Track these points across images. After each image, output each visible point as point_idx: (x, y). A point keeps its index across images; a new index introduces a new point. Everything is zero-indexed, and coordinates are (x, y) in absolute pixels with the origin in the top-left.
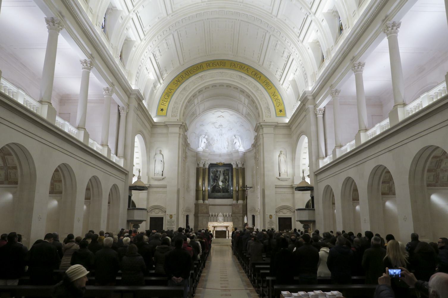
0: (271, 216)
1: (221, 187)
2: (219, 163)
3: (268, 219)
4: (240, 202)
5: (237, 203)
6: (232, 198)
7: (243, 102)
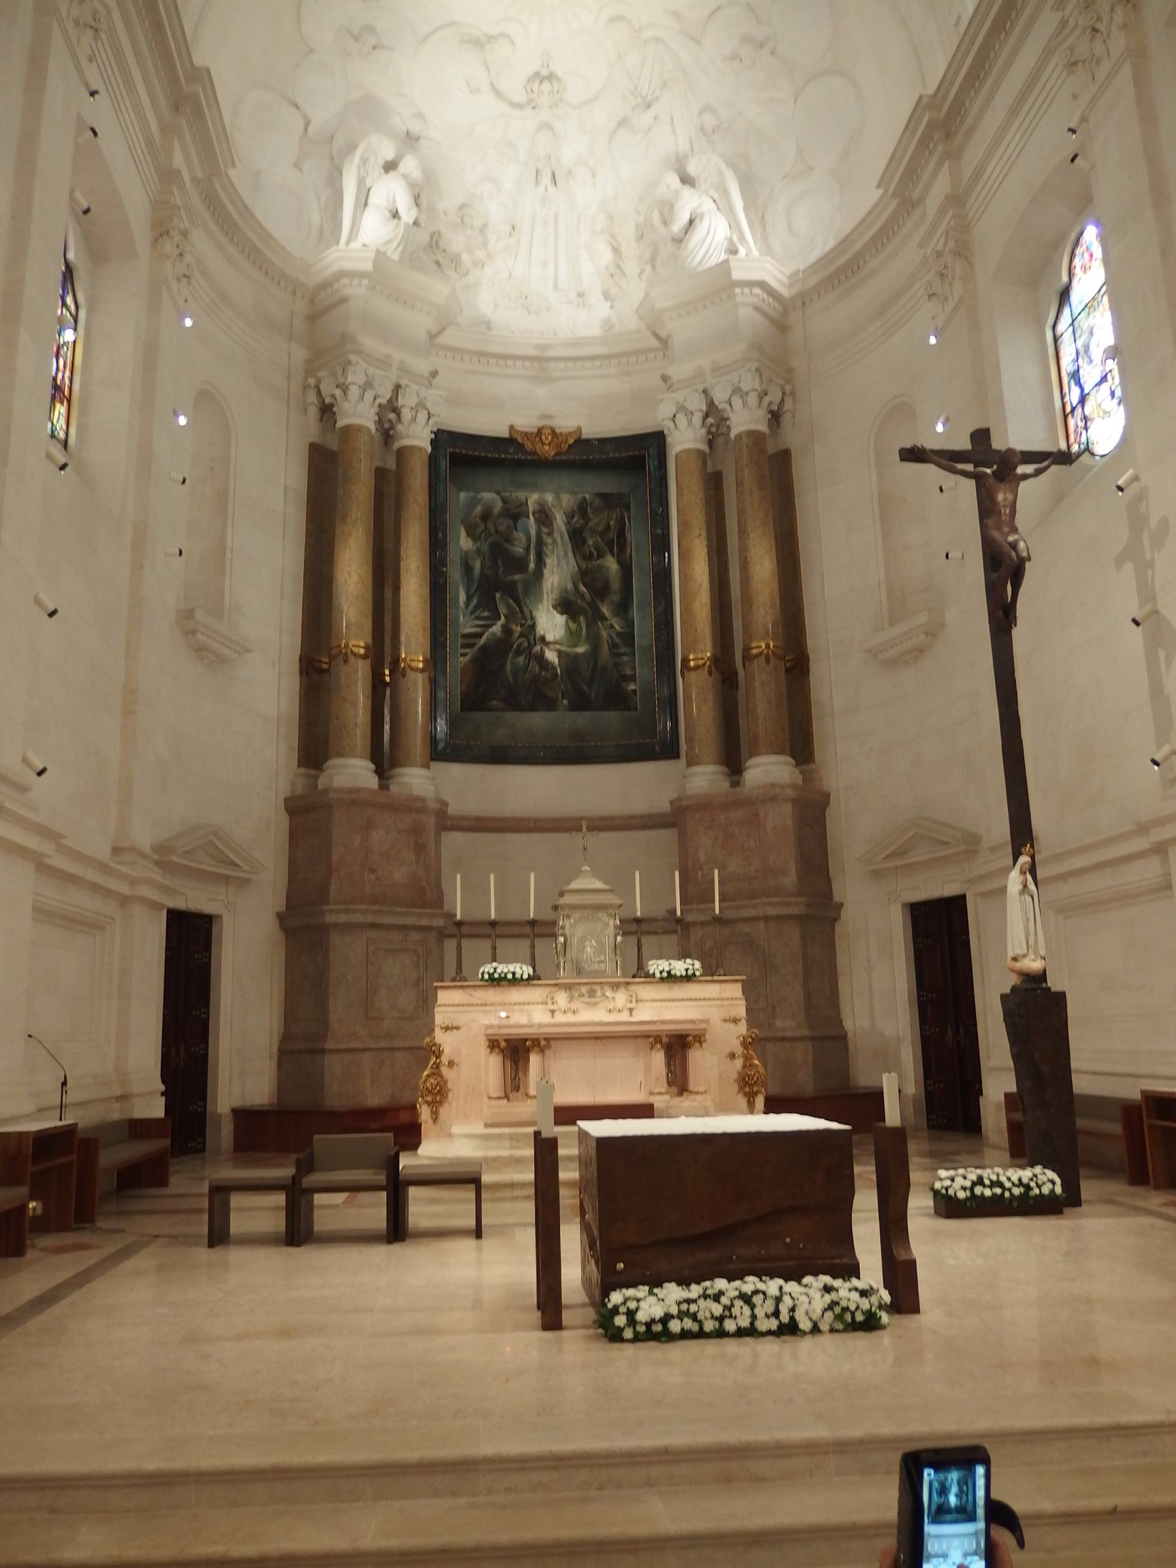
1: (551, 656)
5: (735, 784)
6: (669, 750)
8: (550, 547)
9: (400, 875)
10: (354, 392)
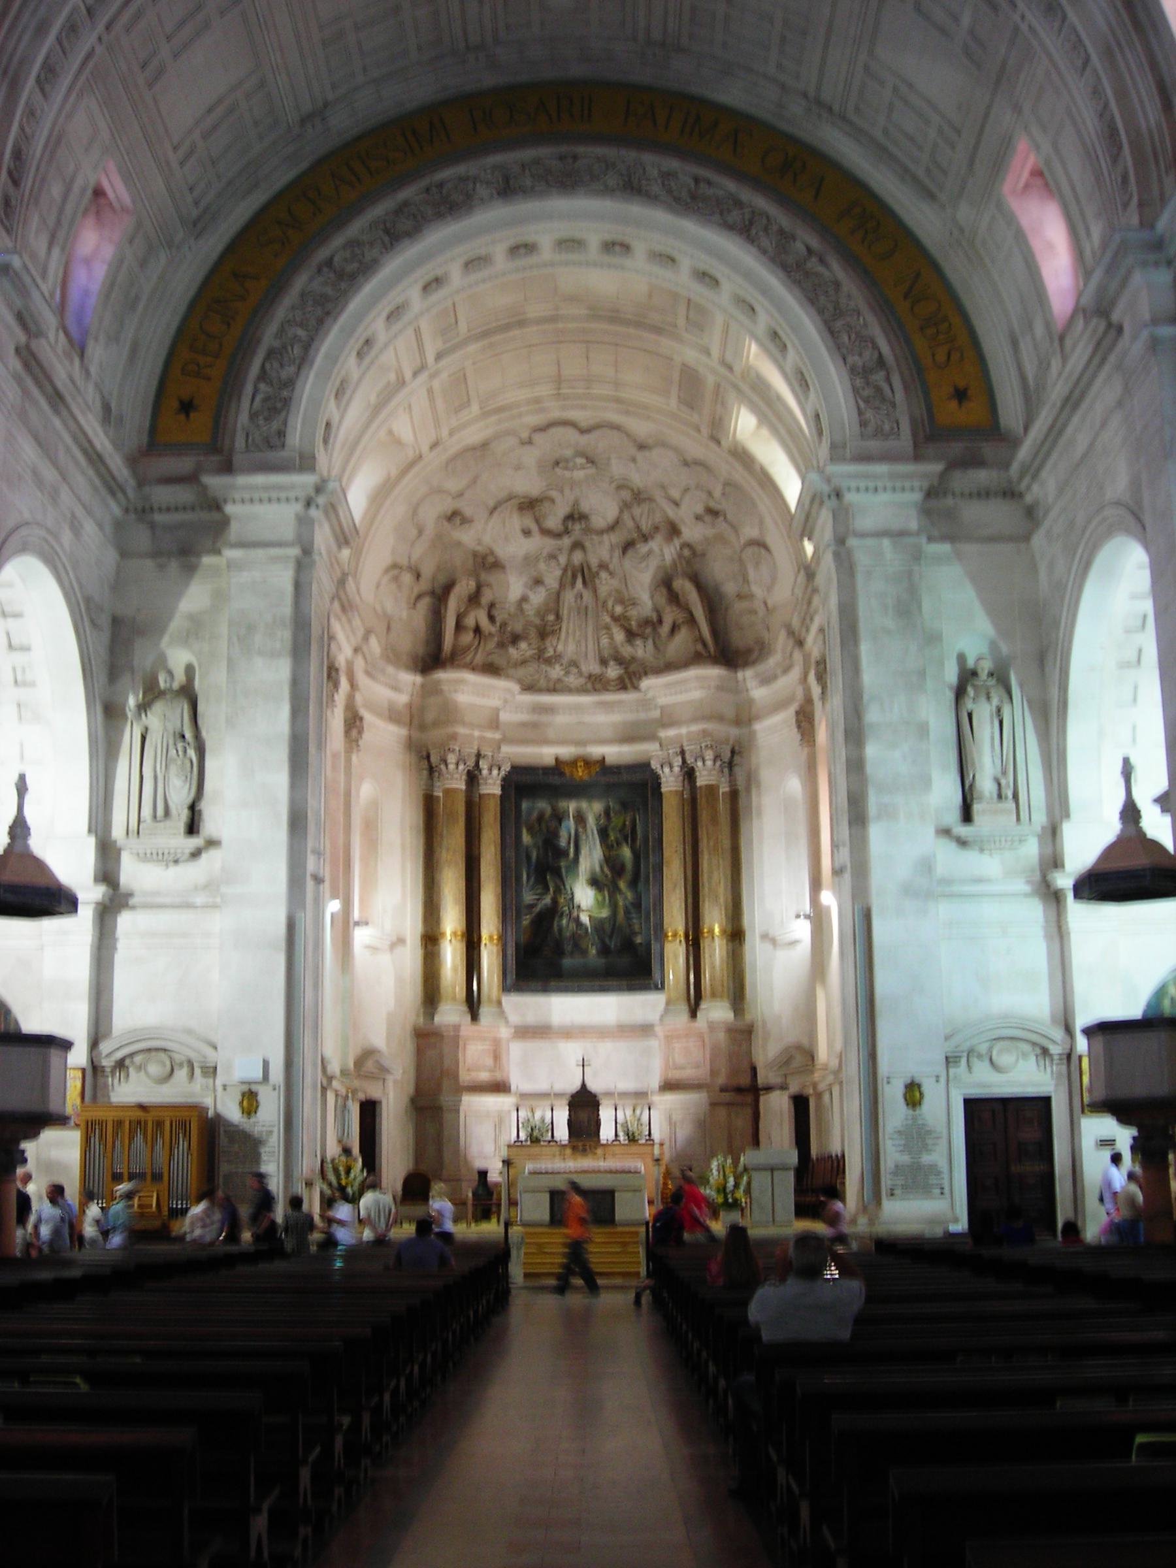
0: (913, 1093)
1: (585, 918)
2: (566, 763)
3: (895, 1112)
4: (717, 1012)
6: (660, 987)
7: (715, 352)
8: (584, 842)
9: (484, 1076)
10: (452, 767)
